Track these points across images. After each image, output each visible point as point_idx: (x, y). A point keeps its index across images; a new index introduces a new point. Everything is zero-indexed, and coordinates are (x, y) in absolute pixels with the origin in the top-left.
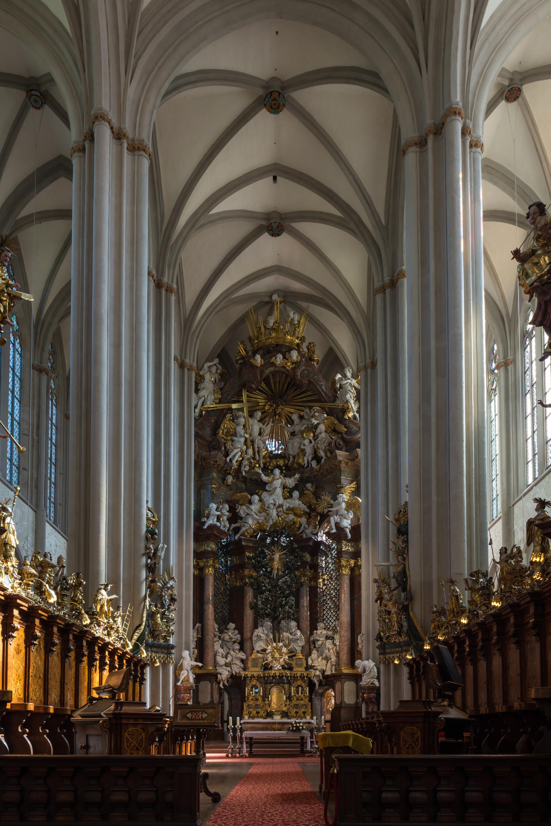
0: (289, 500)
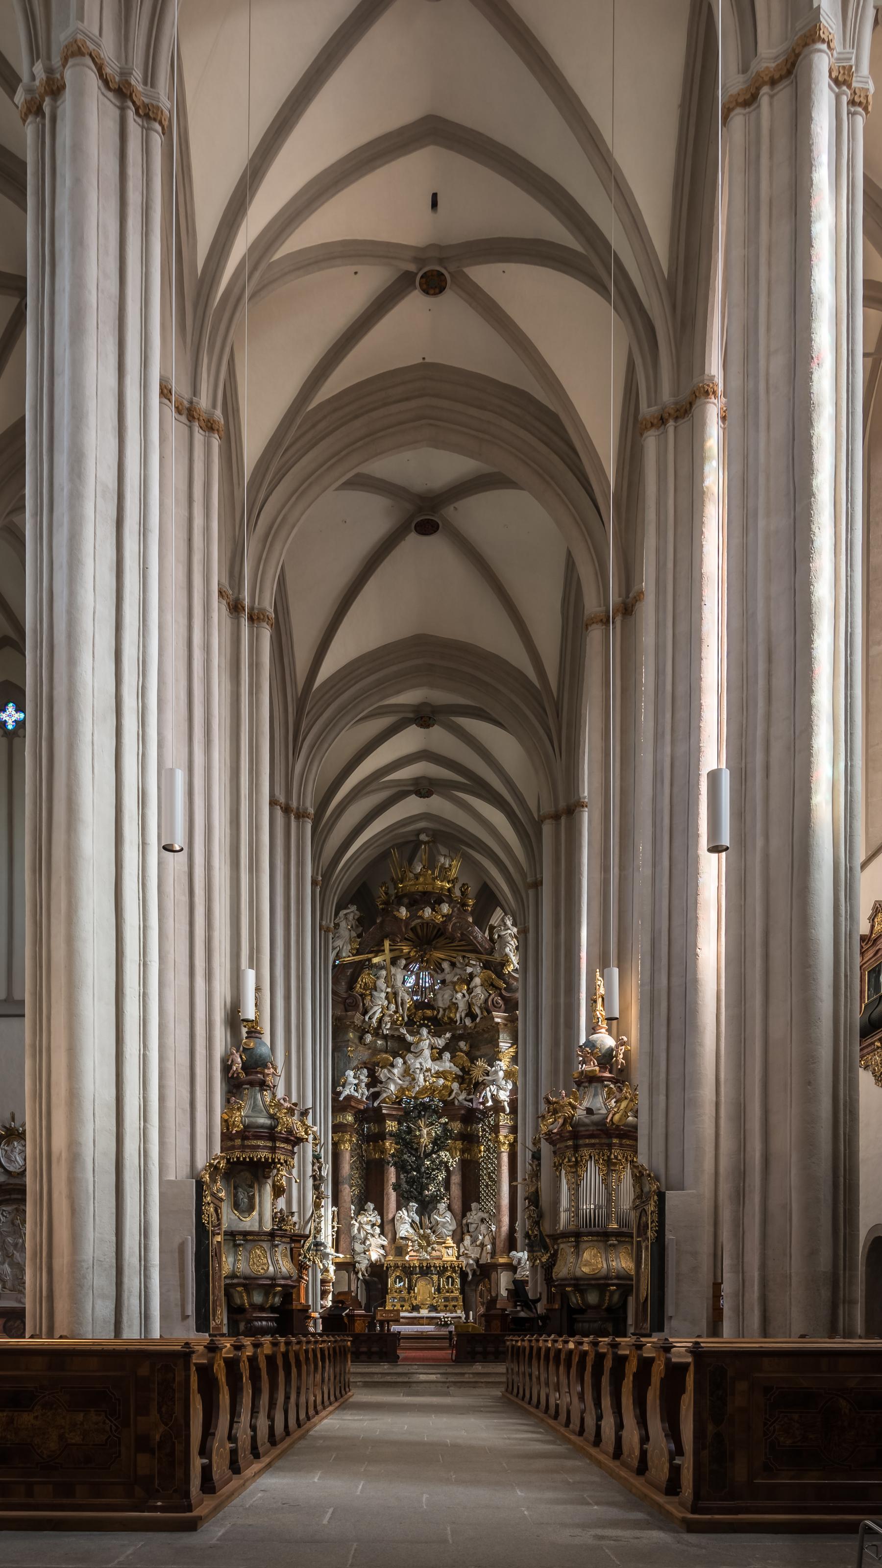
0: (438, 1062)
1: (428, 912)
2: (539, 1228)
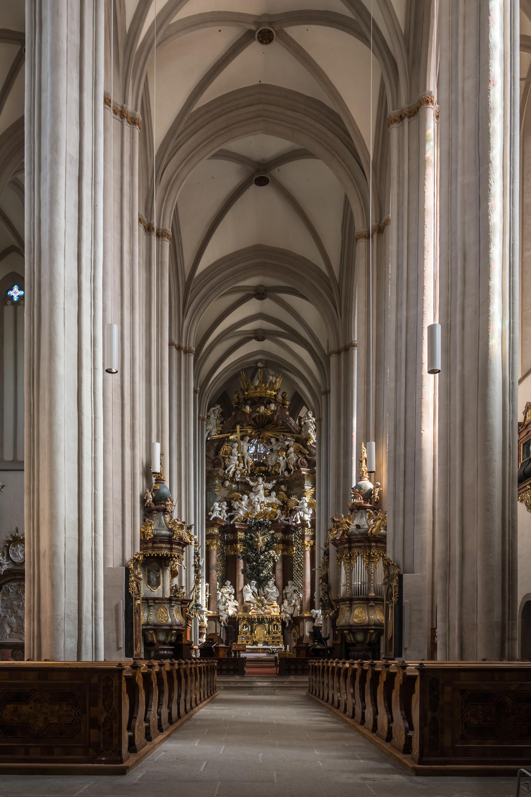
1: (262, 409)
2: (328, 595)
